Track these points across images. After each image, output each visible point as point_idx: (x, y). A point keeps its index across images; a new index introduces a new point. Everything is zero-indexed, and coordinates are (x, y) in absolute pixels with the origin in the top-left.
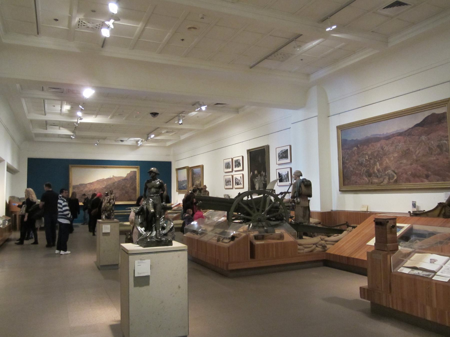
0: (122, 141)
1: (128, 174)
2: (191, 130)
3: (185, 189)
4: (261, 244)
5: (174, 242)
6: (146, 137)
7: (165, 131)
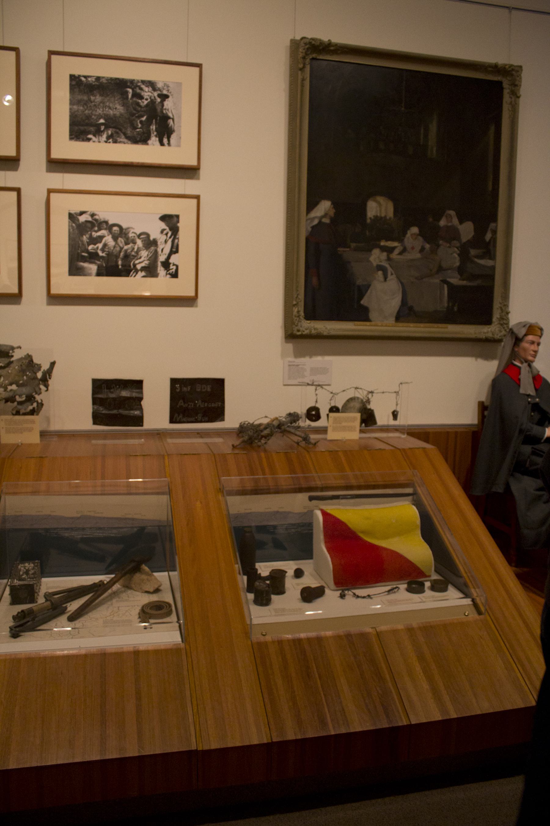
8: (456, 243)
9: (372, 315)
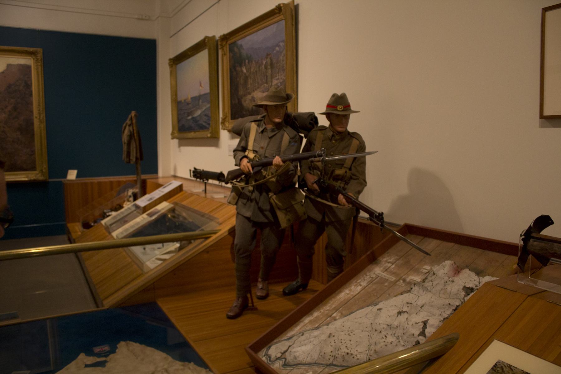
3: (202, 128)
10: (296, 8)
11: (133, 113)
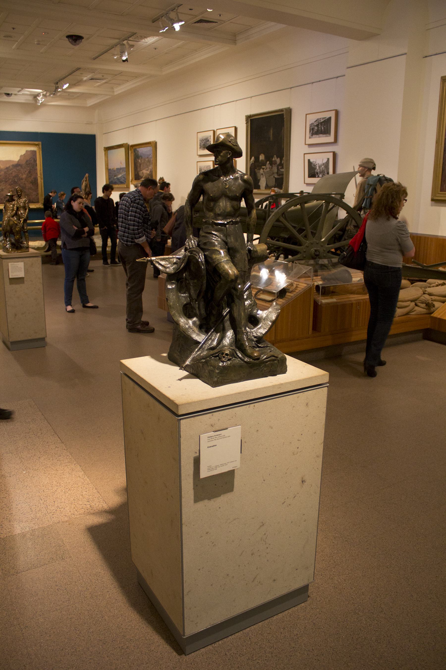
0: (8, 95)
1: (21, 156)
2: (136, 76)
3: (122, 183)
4: (328, 304)
5: (291, 361)
6: (53, 87)
7: (89, 76)
8: (276, 165)
9: (261, 187)
10: (156, 143)
11: (87, 175)
